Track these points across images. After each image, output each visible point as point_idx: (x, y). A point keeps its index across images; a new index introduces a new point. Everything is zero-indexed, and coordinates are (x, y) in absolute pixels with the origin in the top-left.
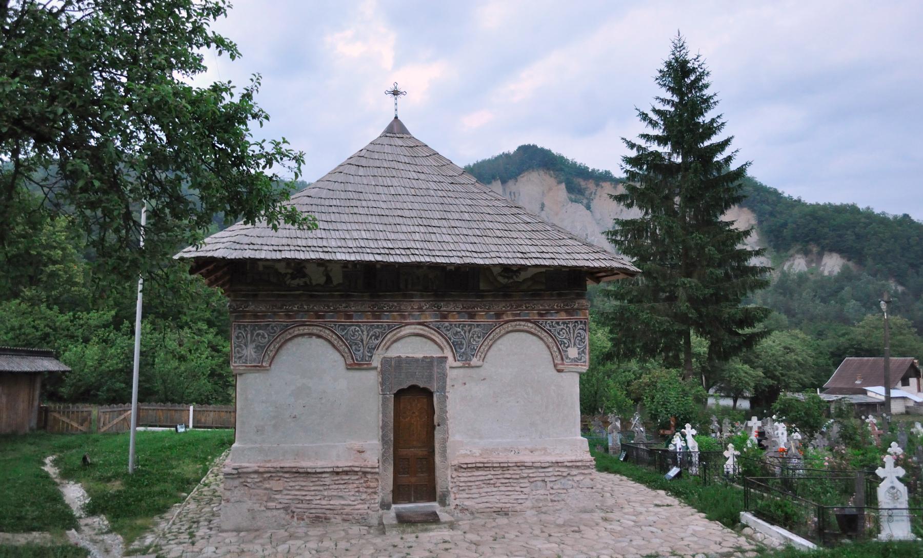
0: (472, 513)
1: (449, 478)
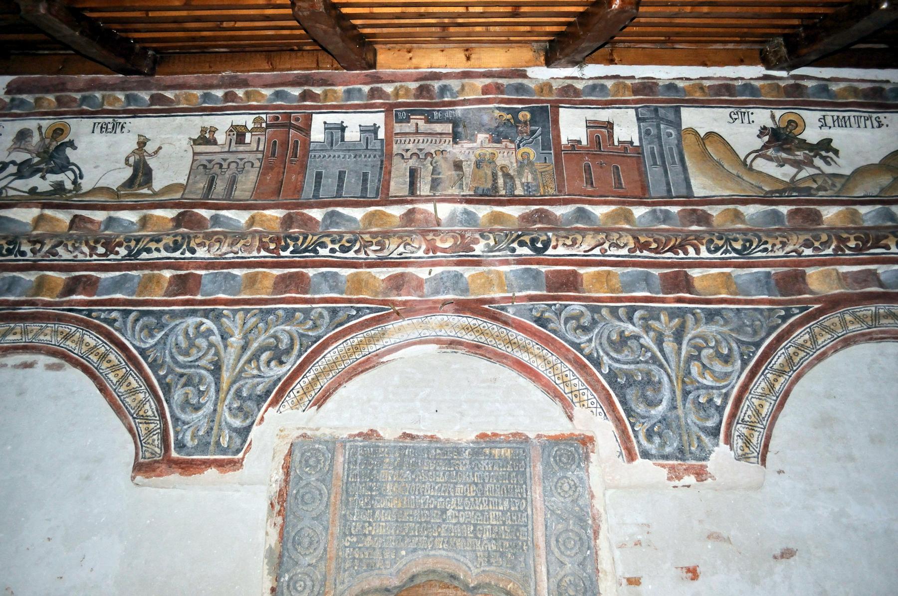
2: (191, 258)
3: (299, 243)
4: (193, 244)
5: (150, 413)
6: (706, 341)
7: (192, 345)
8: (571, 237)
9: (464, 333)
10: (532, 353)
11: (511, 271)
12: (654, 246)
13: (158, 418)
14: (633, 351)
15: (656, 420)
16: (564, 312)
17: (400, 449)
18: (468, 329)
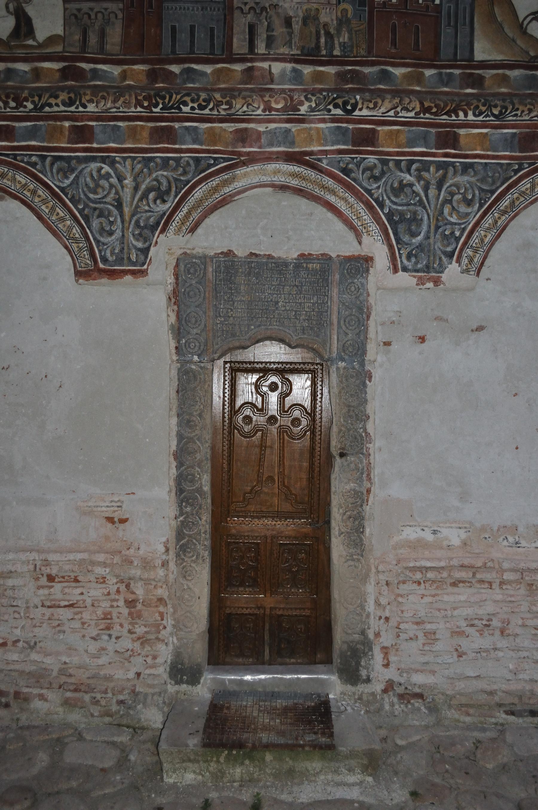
1: (371, 607)
2: (84, 112)
3: (167, 100)
4: (83, 101)
5: (77, 236)
6: (458, 189)
7: (97, 185)
8: (373, 101)
9: (291, 179)
10: (338, 196)
11: (327, 127)
12: (434, 110)
13: (83, 239)
14: (407, 196)
15: (415, 246)
16: (362, 164)
17: (249, 263)
18: (293, 175)
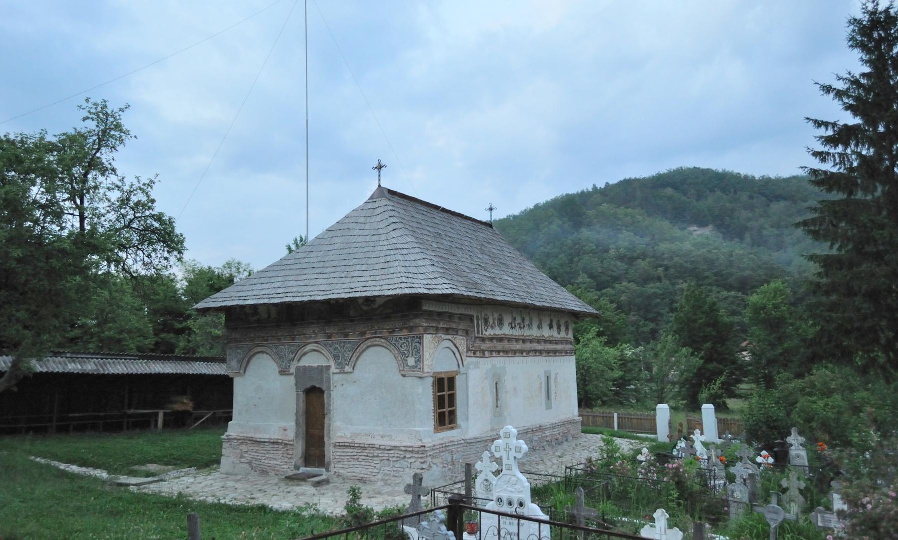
0: (343, 479)
1: (331, 453)
